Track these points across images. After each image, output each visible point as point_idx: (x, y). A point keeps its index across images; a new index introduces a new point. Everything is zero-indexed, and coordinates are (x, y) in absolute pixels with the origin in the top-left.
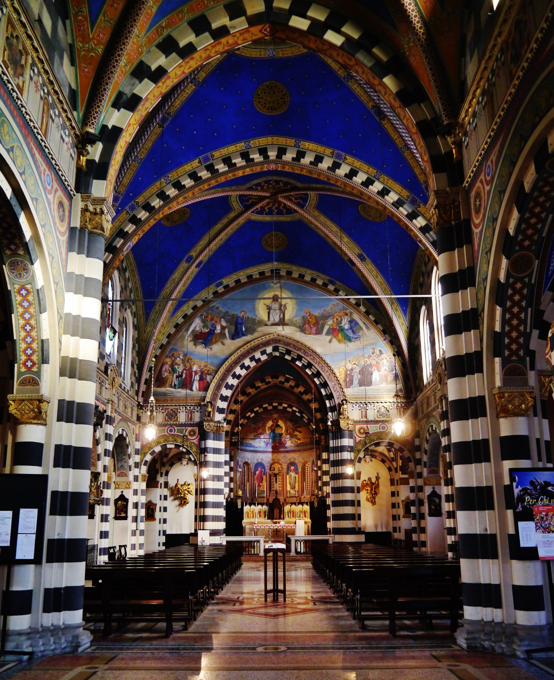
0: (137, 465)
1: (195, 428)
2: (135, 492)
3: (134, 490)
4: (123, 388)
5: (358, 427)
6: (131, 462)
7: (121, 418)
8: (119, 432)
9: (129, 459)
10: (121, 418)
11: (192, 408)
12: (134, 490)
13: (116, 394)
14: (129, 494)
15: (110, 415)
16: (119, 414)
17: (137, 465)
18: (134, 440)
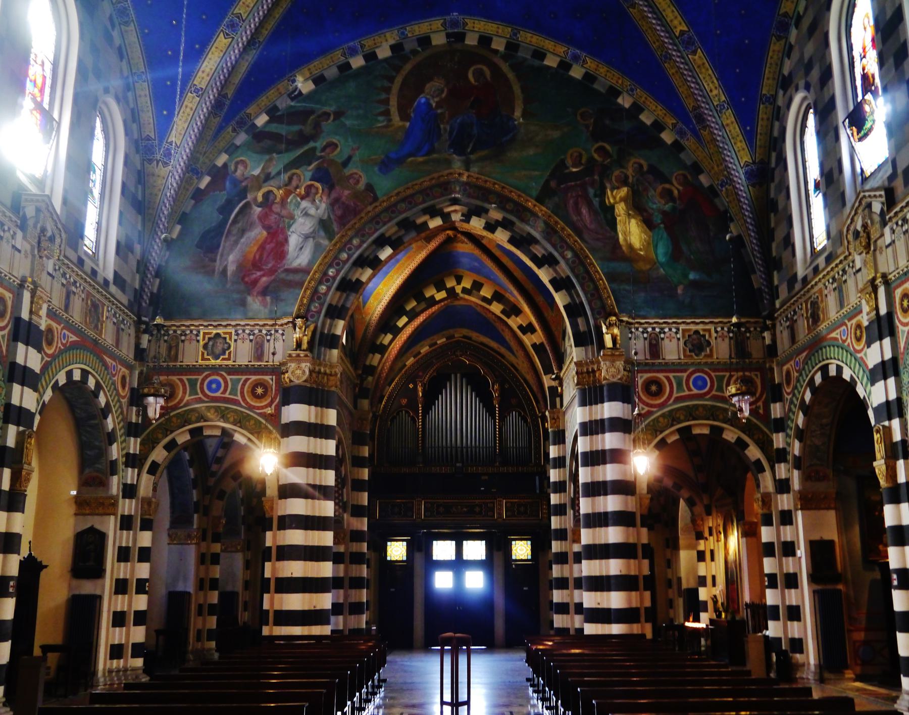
0: (132, 461)
1: (267, 378)
2: (126, 523)
3: (123, 516)
4: (87, 268)
5: (641, 379)
6: (115, 452)
7: (74, 338)
8: (69, 374)
9: (111, 444)
10: (74, 338)
11: (264, 332)
12: (123, 516)
13: (57, 275)
14: (110, 526)
15: (25, 315)
16: (70, 326)
17: (132, 461)
18: (124, 401)
